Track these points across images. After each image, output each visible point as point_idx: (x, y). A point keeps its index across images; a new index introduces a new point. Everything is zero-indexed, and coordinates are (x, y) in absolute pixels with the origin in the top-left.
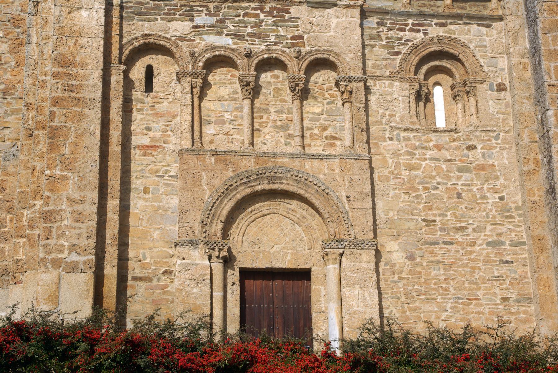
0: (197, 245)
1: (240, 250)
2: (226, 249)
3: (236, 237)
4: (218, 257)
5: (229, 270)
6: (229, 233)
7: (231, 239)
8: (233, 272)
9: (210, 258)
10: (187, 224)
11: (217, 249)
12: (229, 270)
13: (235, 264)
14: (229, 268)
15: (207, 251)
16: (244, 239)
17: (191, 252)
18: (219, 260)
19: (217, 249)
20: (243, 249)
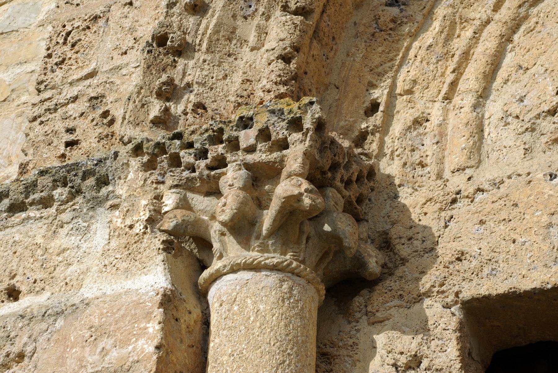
0: (103, 181)
1: (457, 182)
2: (295, 156)
3: (436, 113)
4: (242, 227)
5: (381, 339)
6: (380, 94)
7: (397, 128)
8: (408, 343)
9: (189, 249)
10: (74, 91)
11: (232, 177)
12: (381, 339)
13: (426, 282)
14: (379, 323)
15: (170, 201)
16: (494, 108)
17: (63, 239)
18: (254, 255)
19: (232, 177)
20: (486, 174)
